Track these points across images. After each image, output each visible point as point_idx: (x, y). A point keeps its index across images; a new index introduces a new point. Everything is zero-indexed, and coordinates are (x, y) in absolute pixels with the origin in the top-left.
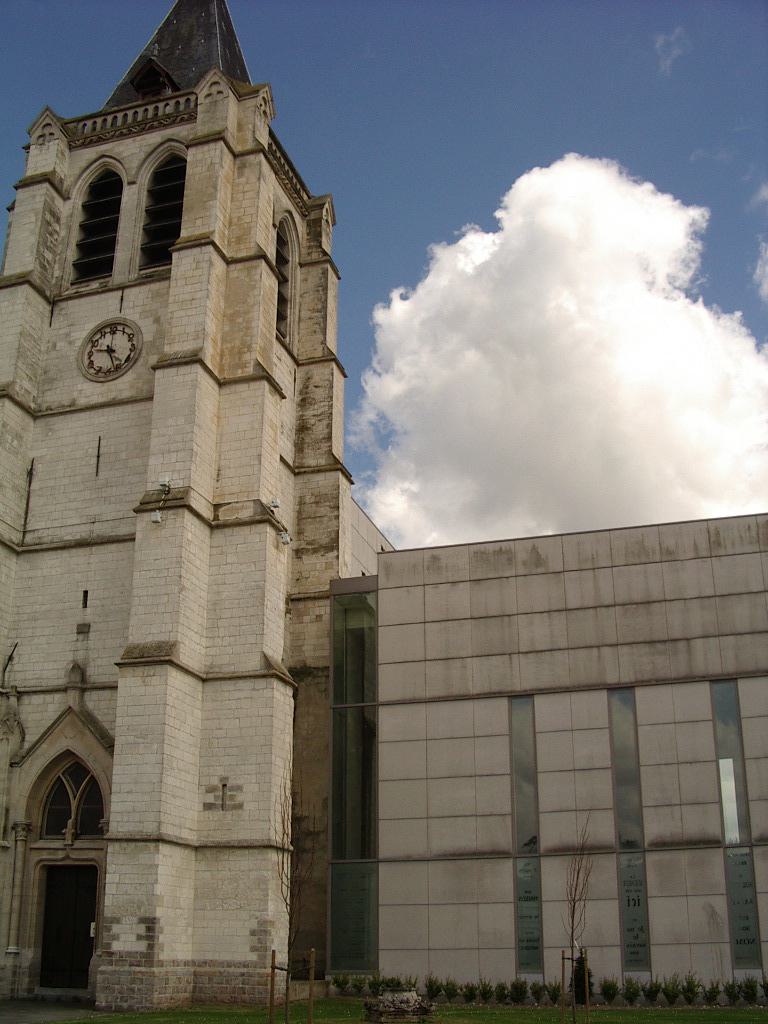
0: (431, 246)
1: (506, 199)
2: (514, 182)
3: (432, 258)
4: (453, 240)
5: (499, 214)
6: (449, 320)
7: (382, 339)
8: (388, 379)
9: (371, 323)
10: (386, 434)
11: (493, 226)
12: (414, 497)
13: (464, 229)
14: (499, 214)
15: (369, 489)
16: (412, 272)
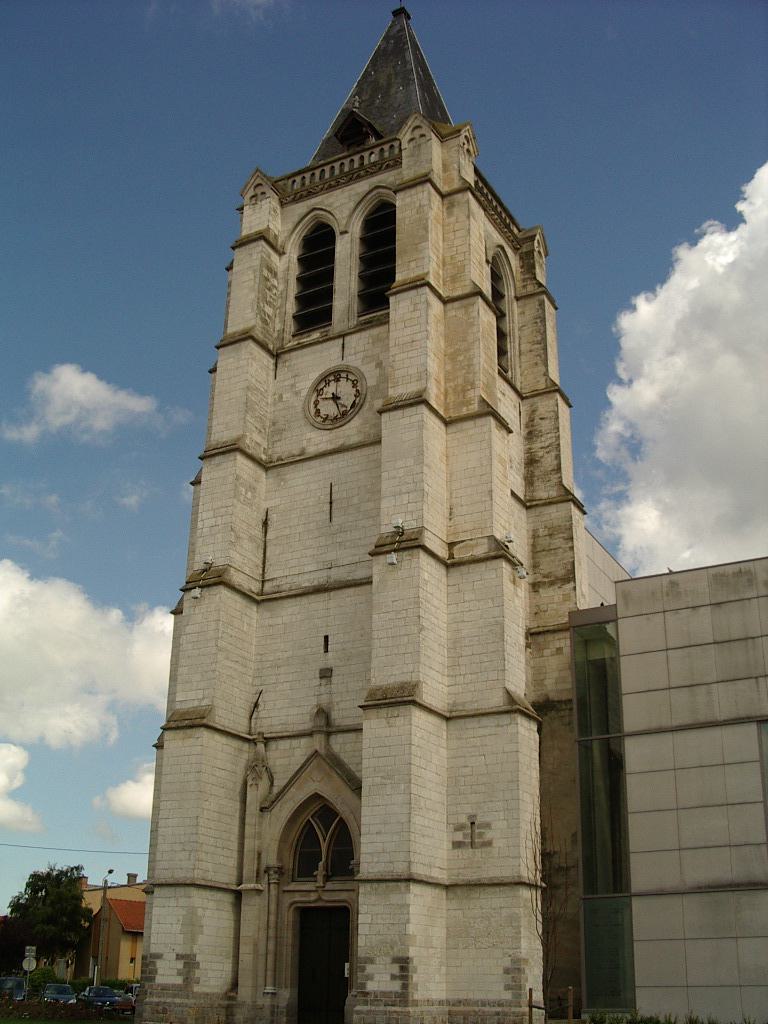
0: (676, 249)
1: (749, 189)
2: (755, 173)
3: (677, 260)
4: (694, 241)
5: (741, 207)
6: (704, 317)
7: (627, 343)
8: (639, 386)
9: (614, 329)
10: (634, 446)
11: (732, 221)
12: (666, 511)
13: (705, 225)
14: (741, 207)
15: (618, 509)
16: (655, 273)
